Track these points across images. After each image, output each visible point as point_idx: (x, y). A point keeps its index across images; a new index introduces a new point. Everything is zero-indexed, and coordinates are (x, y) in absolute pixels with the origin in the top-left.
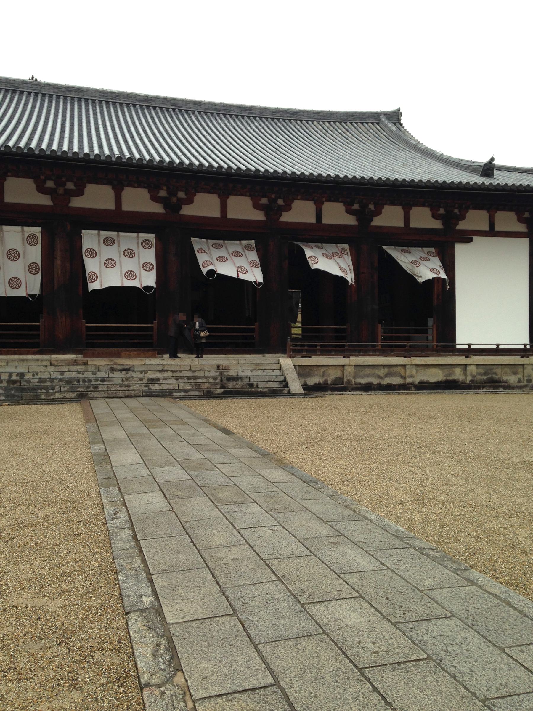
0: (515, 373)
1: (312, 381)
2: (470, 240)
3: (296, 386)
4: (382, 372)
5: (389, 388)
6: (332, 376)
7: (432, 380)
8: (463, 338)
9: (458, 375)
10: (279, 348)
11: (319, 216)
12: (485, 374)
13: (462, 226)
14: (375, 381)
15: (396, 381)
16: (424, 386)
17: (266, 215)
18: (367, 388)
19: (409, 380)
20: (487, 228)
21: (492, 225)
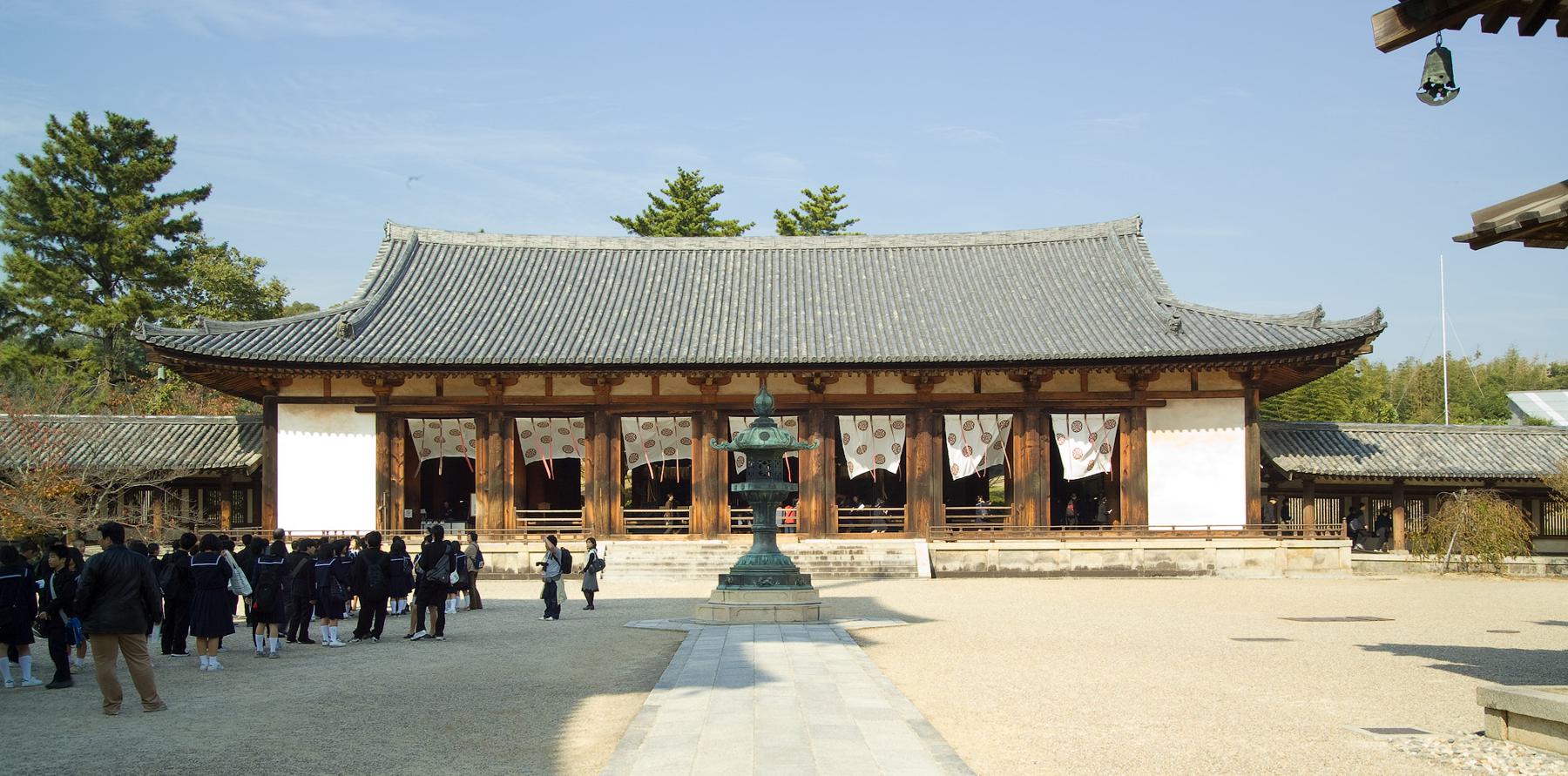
0: (1194, 558)
1: (952, 566)
2: (1163, 404)
3: (925, 570)
4: (1032, 556)
5: (1040, 574)
6: (974, 561)
7: (1091, 566)
8: (1156, 519)
9: (1122, 560)
10: (913, 532)
11: (977, 387)
12: (1156, 559)
13: (1154, 386)
14: (1023, 567)
15: (1048, 567)
16: (1082, 572)
17: (917, 388)
18: (1015, 574)
19: (1063, 566)
20: (1188, 387)
21: (1194, 386)
